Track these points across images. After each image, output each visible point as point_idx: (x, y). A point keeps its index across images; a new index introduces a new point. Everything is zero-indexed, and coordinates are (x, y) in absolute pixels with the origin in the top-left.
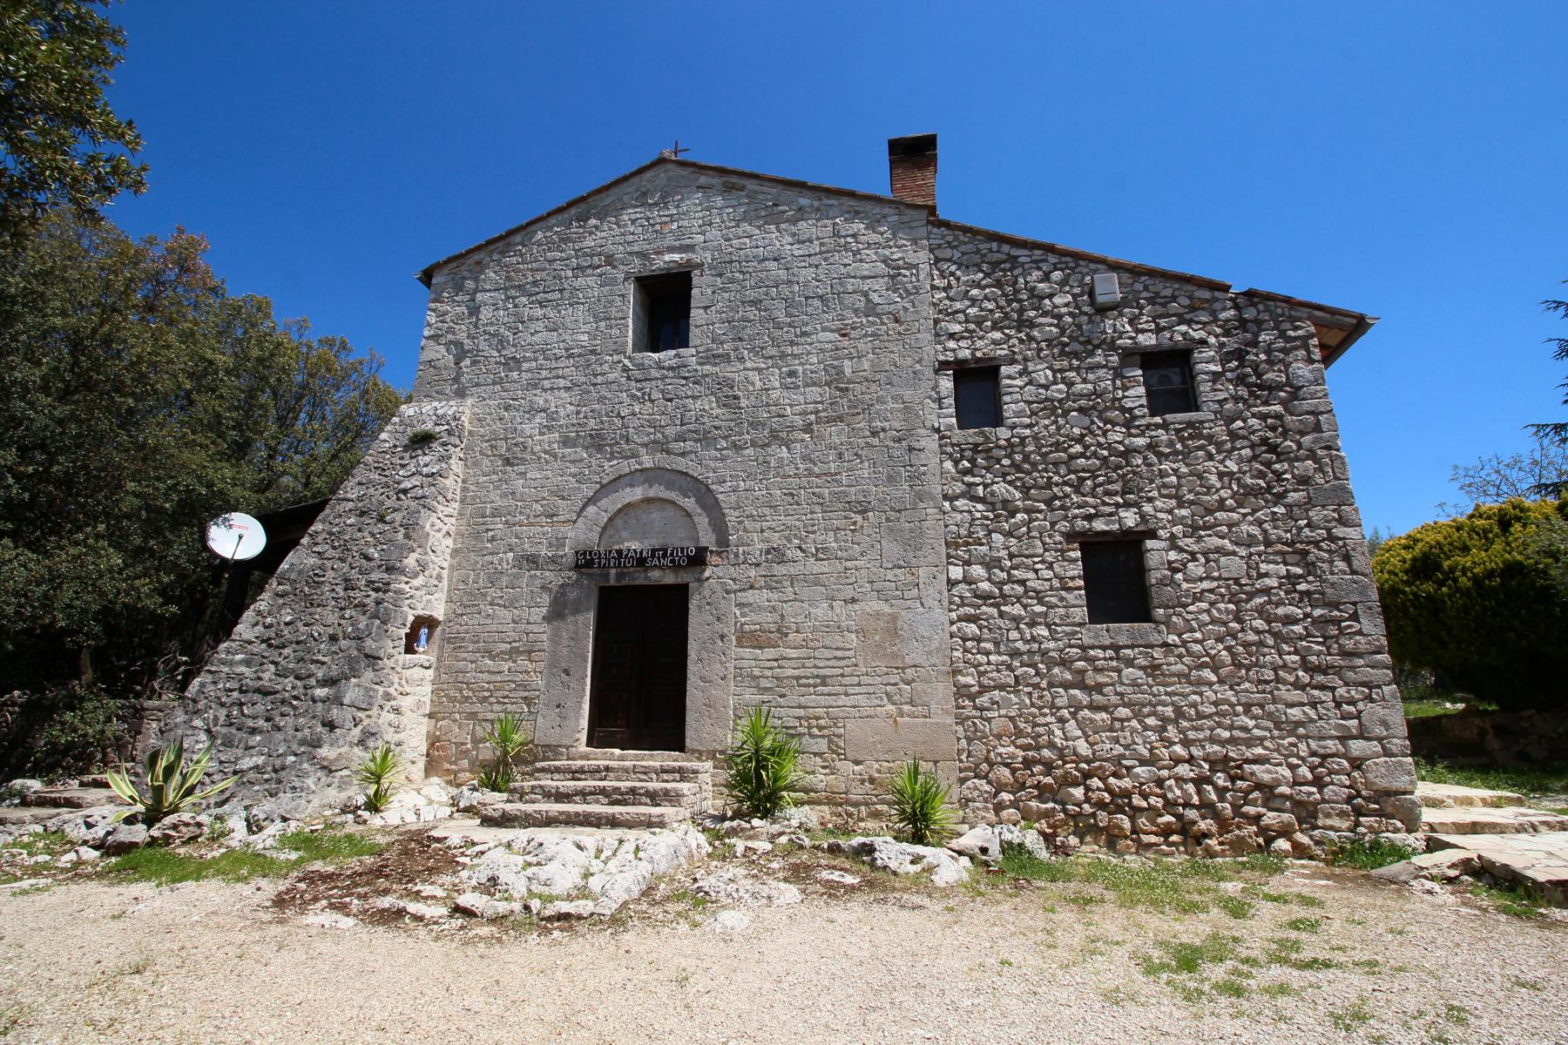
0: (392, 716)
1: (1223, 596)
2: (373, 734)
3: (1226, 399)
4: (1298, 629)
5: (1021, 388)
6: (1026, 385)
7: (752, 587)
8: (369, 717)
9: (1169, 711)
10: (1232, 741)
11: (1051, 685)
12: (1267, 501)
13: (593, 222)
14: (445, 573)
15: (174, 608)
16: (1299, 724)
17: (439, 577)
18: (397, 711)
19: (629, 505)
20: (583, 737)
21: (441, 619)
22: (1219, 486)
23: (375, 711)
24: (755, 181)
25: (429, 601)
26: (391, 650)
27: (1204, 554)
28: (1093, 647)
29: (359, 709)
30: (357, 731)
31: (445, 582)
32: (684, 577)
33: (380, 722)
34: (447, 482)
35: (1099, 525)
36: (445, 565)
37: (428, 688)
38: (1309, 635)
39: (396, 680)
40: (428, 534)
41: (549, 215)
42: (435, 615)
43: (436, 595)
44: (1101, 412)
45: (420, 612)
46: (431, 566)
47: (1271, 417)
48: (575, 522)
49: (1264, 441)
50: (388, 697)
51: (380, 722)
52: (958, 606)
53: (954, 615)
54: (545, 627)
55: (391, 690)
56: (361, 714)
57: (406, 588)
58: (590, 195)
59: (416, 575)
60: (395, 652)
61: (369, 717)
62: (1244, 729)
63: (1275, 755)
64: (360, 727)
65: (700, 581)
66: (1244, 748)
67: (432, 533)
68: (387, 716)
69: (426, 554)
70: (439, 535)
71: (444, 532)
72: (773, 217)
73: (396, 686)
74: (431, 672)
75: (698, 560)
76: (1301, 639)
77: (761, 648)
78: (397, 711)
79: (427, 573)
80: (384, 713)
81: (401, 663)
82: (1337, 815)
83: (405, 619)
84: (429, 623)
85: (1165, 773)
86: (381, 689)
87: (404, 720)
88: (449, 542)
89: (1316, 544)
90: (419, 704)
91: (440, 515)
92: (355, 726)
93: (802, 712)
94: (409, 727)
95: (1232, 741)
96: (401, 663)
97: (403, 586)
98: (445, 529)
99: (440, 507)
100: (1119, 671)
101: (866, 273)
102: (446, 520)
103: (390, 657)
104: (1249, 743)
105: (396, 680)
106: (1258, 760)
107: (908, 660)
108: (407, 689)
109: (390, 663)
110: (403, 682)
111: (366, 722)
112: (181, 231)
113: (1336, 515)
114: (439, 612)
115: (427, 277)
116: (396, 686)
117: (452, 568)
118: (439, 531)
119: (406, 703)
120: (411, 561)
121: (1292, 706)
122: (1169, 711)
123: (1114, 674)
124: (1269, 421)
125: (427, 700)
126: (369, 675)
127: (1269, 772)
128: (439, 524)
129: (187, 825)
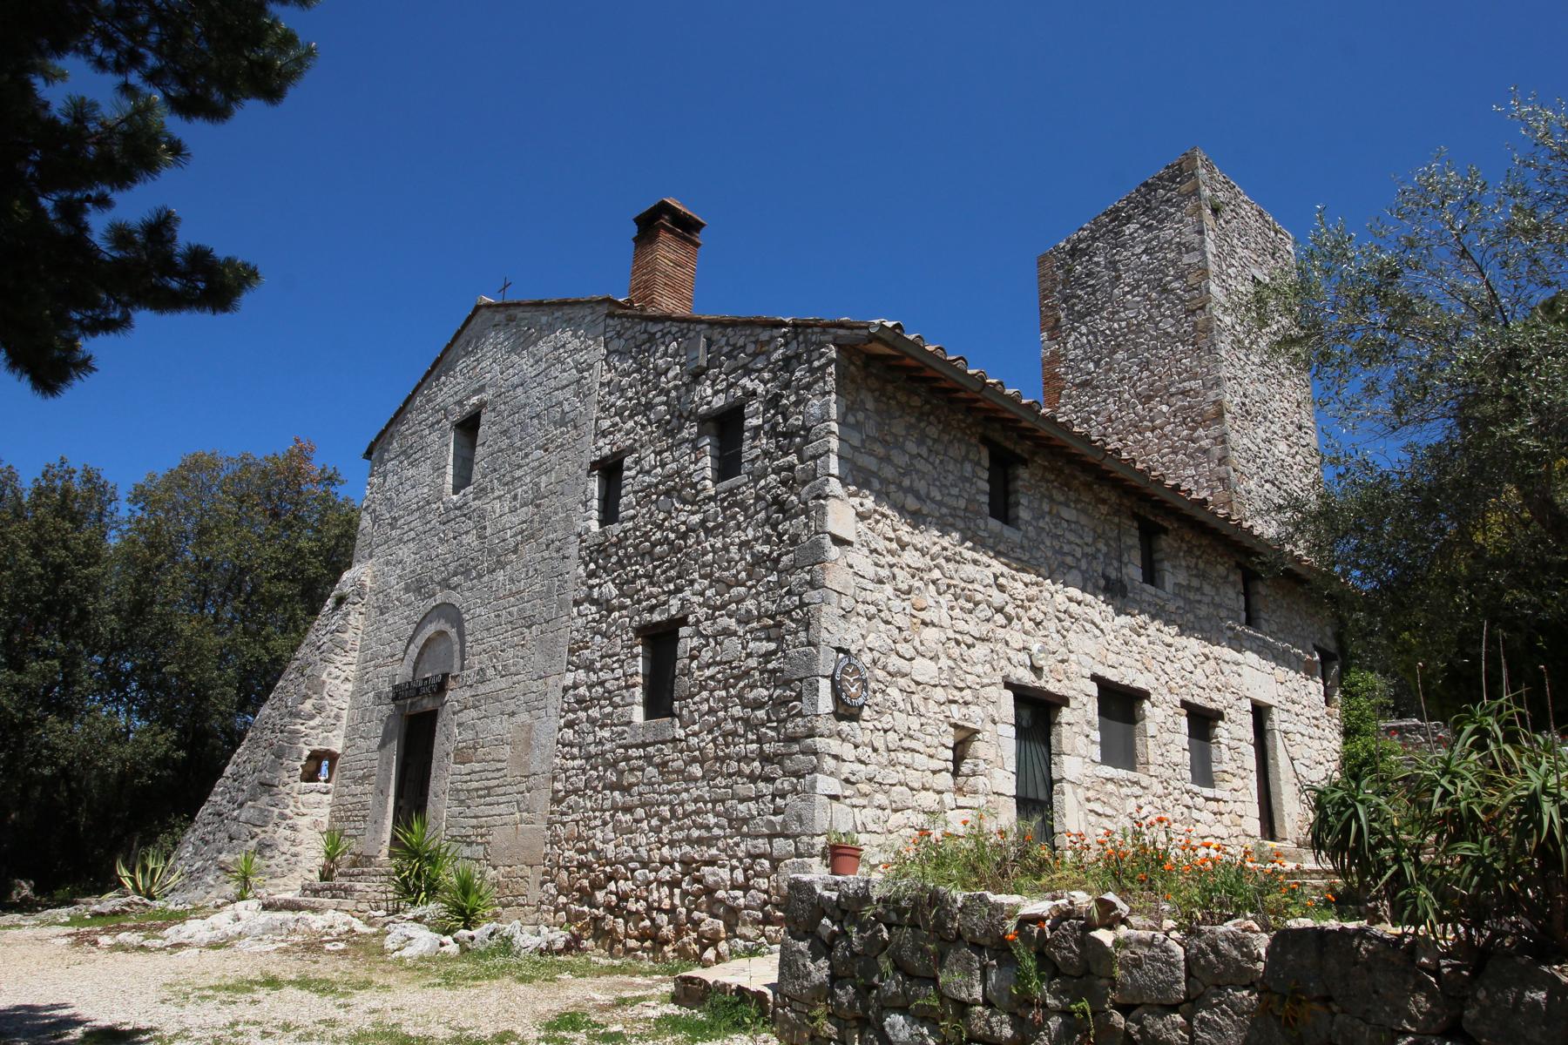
0: (288, 832)
1: (719, 682)
2: (268, 846)
3: (757, 457)
4: (761, 714)
5: (634, 478)
6: (638, 473)
7: (466, 708)
8: (265, 832)
9: (665, 811)
10: (700, 841)
11: (604, 788)
12: (767, 569)
13: (443, 378)
14: (345, 714)
15: (182, 754)
16: (745, 821)
17: (337, 717)
18: (293, 828)
19: (429, 640)
20: (385, 851)
21: (339, 752)
22: (737, 558)
23: (270, 827)
24: (521, 309)
25: (327, 737)
26: (286, 780)
27: (715, 637)
28: (631, 746)
29: (255, 826)
30: (253, 843)
31: (344, 721)
32: (427, 704)
33: (276, 836)
34: (345, 636)
35: (656, 617)
36: (344, 706)
37: (328, 810)
38: (770, 720)
39: (291, 803)
40: (324, 682)
41: (424, 380)
42: (333, 748)
43: (335, 733)
44: (679, 492)
45: (317, 747)
46: (328, 708)
47: (785, 470)
48: (402, 660)
49: (776, 498)
50: (283, 817)
51: (276, 836)
52: (567, 712)
53: (562, 721)
54: (376, 755)
55: (287, 811)
56: (256, 830)
57: (302, 728)
58: (442, 355)
59: (312, 717)
60: (290, 780)
61: (265, 832)
62: (708, 828)
63: (723, 855)
64: (256, 840)
65: (443, 705)
66: (705, 848)
67: (329, 681)
68: (283, 832)
69: (322, 698)
70: (337, 681)
71: (342, 678)
72: (523, 343)
73: (292, 808)
74: (329, 797)
75: (441, 688)
76: (763, 725)
77: (463, 763)
78: (293, 828)
79: (323, 715)
80: (281, 830)
81: (296, 789)
82: (751, 923)
83: (301, 753)
84: (332, 757)
85: (652, 876)
86: (276, 811)
87: (300, 836)
88: (349, 686)
89: (788, 613)
90: (316, 824)
91: (339, 665)
92: (252, 838)
93: (474, 822)
94: (305, 841)
95: (700, 841)
96: (296, 789)
97: (298, 727)
98: (343, 675)
99: (339, 658)
100: (643, 770)
101: (565, 383)
102: (345, 668)
103: (285, 784)
104: (709, 842)
105: (291, 803)
106: (712, 862)
107: (532, 771)
108: (303, 810)
109: (287, 788)
110: (300, 805)
111: (262, 836)
112: (297, 441)
113: (808, 578)
114: (337, 745)
115: (368, 454)
116: (292, 808)
117: (351, 708)
118: (337, 678)
119: (302, 822)
120: (308, 706)
121: (742, 801)
122: (665, 811)
123: (639, 774)
124: (783, 474)
125: (326, 820)
126: (265, 799)
127: (714, 874)
128: (337, 672)
129: (137, 904)
